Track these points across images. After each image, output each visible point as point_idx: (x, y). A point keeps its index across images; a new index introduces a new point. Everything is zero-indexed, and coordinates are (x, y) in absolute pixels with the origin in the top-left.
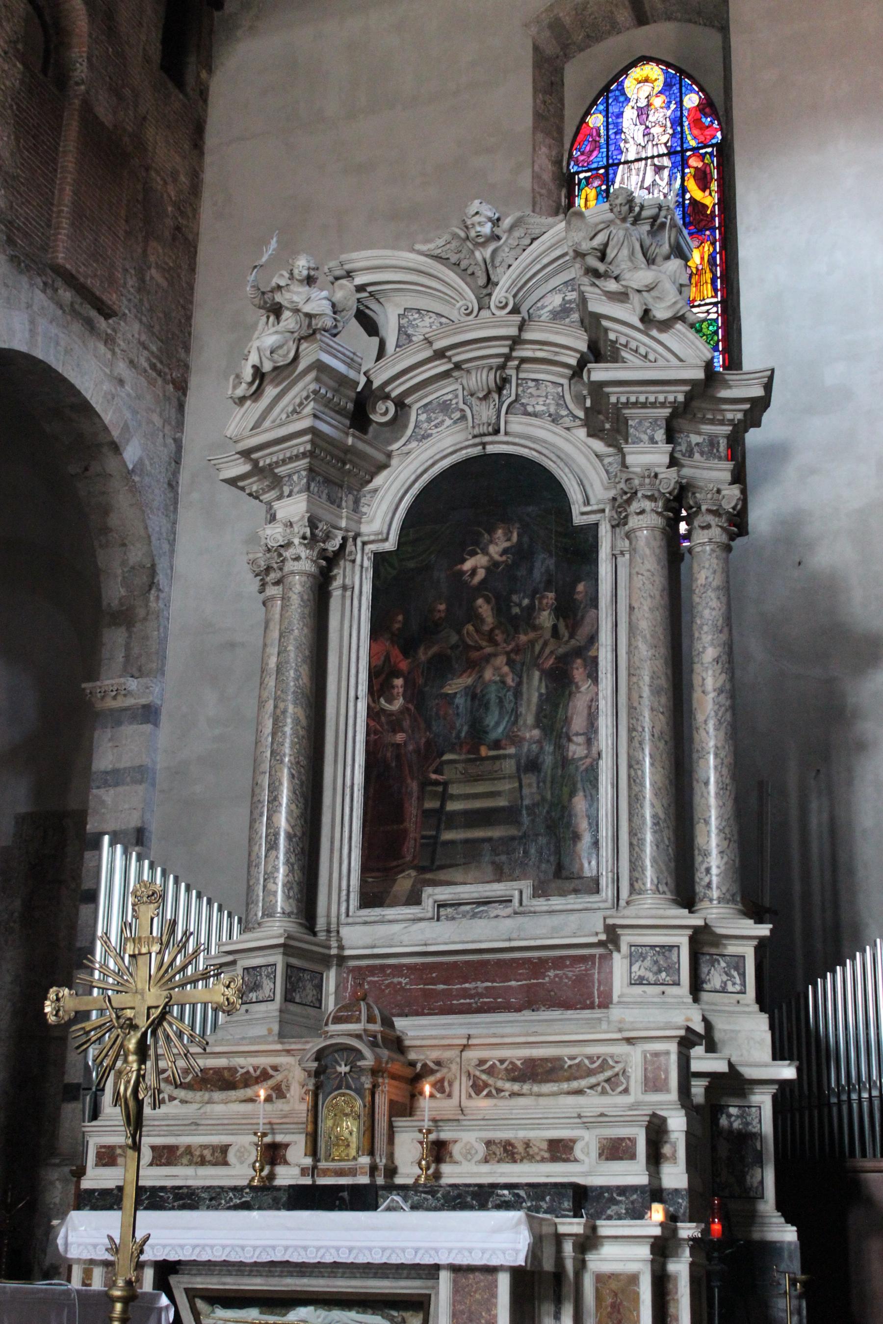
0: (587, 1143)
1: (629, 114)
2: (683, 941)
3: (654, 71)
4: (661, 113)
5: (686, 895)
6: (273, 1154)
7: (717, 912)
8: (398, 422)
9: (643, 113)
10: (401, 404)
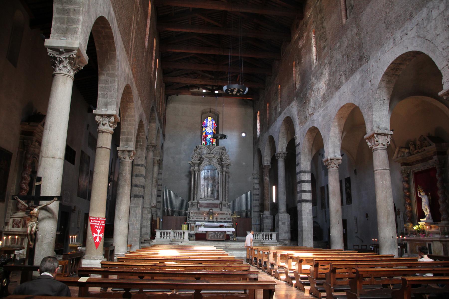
0: (227, 219)
1: (208, 122)
3: (211, 118)
4: (211, 123)
5: (225, 201)
6: (205, 218)
7: (227, 202)
9: (210, 122)
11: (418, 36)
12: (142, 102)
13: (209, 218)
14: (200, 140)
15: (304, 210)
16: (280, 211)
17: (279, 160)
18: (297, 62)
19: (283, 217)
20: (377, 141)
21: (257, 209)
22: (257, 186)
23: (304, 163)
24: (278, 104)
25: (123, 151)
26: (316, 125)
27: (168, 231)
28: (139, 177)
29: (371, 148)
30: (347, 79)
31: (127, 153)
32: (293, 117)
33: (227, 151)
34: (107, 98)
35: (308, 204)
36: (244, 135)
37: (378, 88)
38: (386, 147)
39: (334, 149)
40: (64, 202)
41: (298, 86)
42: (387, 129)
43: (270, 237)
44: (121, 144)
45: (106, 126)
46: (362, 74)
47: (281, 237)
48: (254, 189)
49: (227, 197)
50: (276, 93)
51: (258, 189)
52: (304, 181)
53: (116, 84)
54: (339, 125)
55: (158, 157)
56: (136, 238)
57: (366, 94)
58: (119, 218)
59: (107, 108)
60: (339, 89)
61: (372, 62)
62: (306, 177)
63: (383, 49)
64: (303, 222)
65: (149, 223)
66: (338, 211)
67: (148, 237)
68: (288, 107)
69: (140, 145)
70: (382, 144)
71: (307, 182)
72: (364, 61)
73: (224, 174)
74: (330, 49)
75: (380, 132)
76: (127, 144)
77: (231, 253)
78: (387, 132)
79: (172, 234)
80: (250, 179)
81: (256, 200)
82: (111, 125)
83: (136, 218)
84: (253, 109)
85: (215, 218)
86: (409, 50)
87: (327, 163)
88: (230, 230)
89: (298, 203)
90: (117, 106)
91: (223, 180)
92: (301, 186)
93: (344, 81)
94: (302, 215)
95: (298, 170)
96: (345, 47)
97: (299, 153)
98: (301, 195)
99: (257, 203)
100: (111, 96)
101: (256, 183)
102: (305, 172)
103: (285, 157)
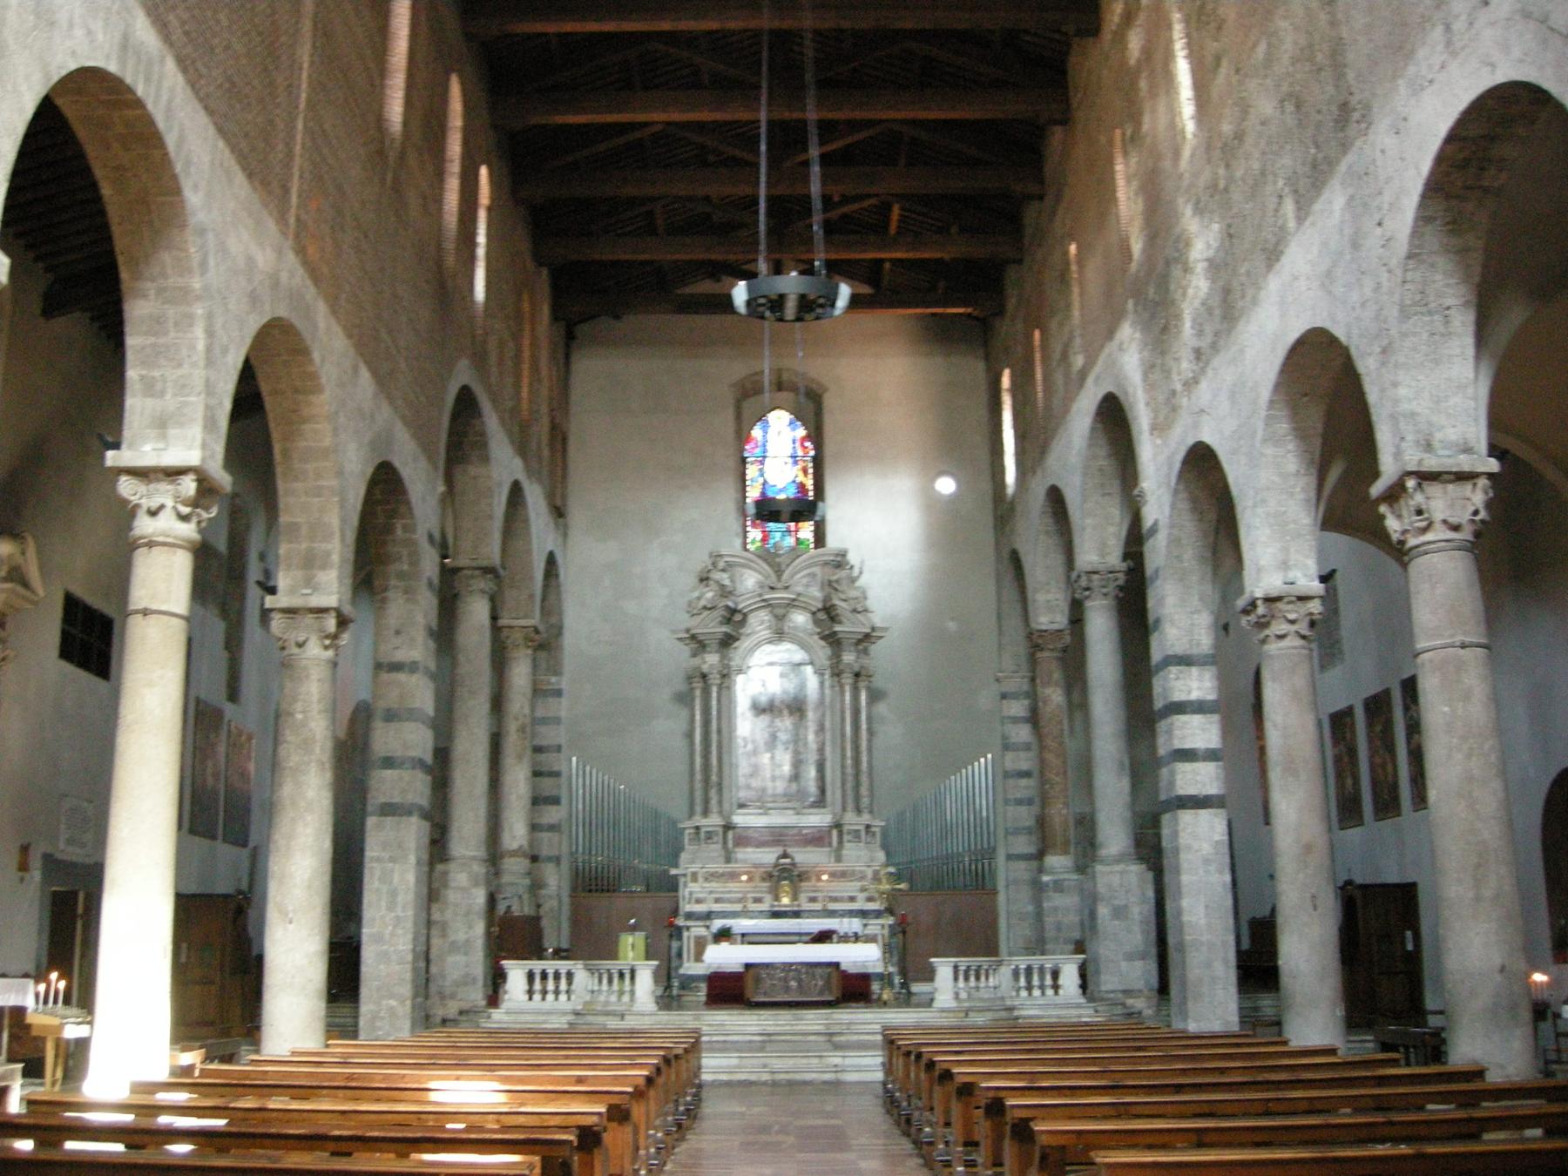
2: (862, 828)
5: (859, 811)
8: (743, 622)
10: (745, 615)
11: (1523, 10)
12: (383, 381)
13: (777, 898)
14: (737, 527)
15: (1189, 848)
16: (1103, 852)
17: (1088, 604)
18: (1129, 133)
19: (1116, 880)
20: (1419, 512)
21: (1024, 845)
22: (1023, 733)
23: (1182, 618)
24: (1071, 339)
25: (291, 612)
26: (1207, 439)
27: (563, 966)
28: (400, 720)
29: (1402, 543)
30: (1303, 211)
31: (309, 619)
32: (1126, 393)
33: (856, 572)
34: (162, 393)
35: (1204, 814)
36: (946, 486)
37: (1410, 256)
38: (1466, 535)
39: (1286, 550)
40: (62, 846)
41: (1137, 247)
42: (1468, 450)
43: (1048, 981)
44: (283, 581)
45: (162, 515)
46: (1350, 191)
47: (1108, 982)
48: (1007, 746)
49: (864, 791)
50: (1063, 278)
51: (1027, 747)
52: (1180, 708)
53: (199, 333)
54: (1301, 434)
55: (526, 617)
56: (393, 1003)
57: (1368, 291)
58: (283, 913)
59: (164, 437)
60: (1278, 260)
61: (1381, 136)
62: (1195, 685)
63: (1412, 70)
64: (1185, 903)
65: (480, 928)
66: (1308, 848)
67: (477, 996)
68: (1106, 351)
69: (401, 576)
70: (1445, 522)
71: (1199, 707)
72: (1352, 129)
73: (848, 680)
74: (1238, 71)
75: (1431, 464)
76: (309, 582)
77: (837, 1061)
78: (1465, 463)
79: (582, 977)
80: (985, 699)
81: (1019, 802)
82: (186, 510)
83: (391, 906)
84: (987, 358)
85: (803, 897)
86: (1501, 77)
87: (1252, 618)
88: (863, 956)
89: (1166, 811)
90: (210, 424)
91: (843, 712)
92: (1170, 732)
93: (1292, 224)
94: (1177, 871)
95: (1156, 656)
96: (1286, 59)
97: (1157, 571)
98: (1172, 774)
99: (1025, 816)
100: (183, 388)
101: (1015, 720)
102: (1185, 661)
103: (1121, 588)
